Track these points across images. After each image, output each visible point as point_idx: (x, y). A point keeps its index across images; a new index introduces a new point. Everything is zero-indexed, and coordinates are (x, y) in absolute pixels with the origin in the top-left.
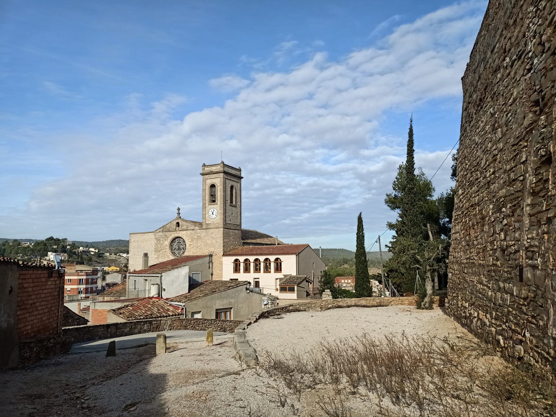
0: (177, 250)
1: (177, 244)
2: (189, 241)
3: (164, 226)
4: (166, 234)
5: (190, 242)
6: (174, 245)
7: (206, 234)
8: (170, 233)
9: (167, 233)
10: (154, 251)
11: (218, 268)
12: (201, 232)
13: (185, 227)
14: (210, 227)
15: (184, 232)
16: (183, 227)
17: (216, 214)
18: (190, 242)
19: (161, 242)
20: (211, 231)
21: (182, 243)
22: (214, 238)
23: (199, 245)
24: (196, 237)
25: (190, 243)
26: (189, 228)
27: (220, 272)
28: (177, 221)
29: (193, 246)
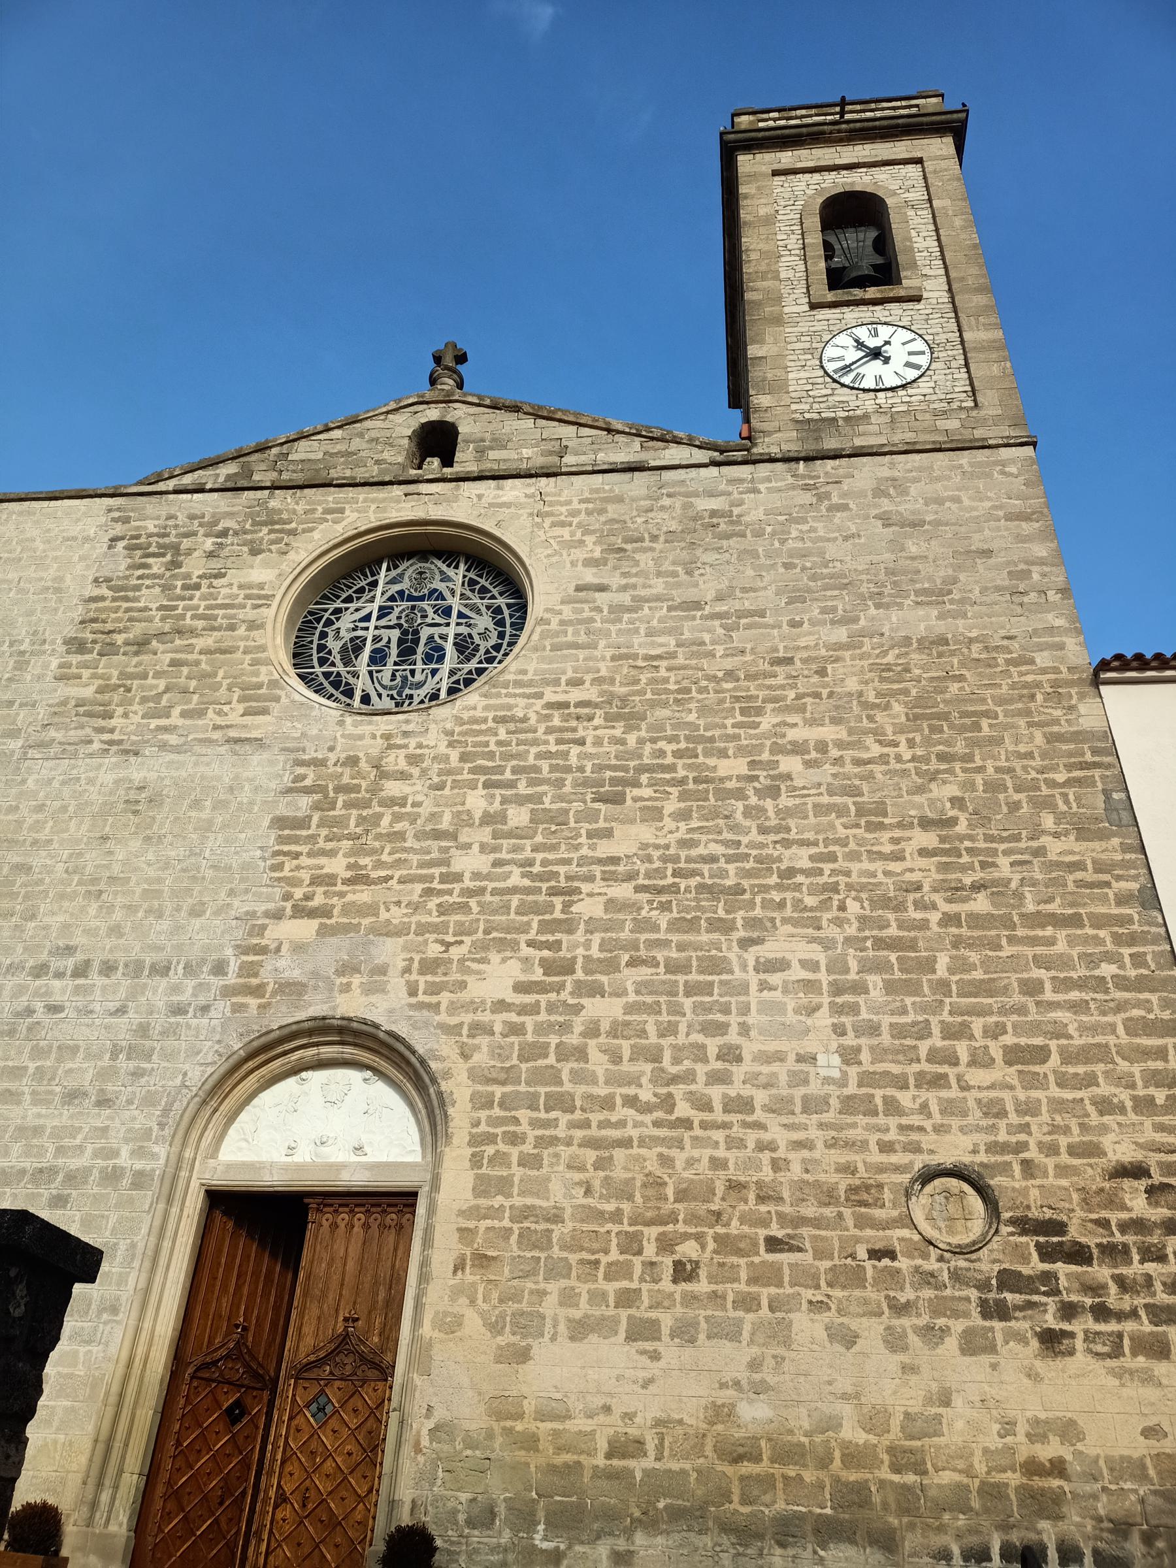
0: (378, 657)
1: (384, 612)
2: (579, 554)
3: (262, 449)
4: (273, 504)
5: (589, 562)
6: (345, 623)
7: (808, 498)
8: (332, 496)
9: (279, 501)
10: (68, 642)
11: (1047, 804)
12: (731, 482)
13: (526, 452)
14: (858, 442)
15: (513, 490)
16: (492, 454)
17: (923, 360)
18: (589, 562)
19: (195, 566)
20: (867, 471)
21: (456, 604)
22: (917, 524)
23: (707, 588)
24: (674, 526)
25: (590, 576)
26: (569, 459)
27: (1111, 849)
28: (433, 414)
29: (626, 598)
